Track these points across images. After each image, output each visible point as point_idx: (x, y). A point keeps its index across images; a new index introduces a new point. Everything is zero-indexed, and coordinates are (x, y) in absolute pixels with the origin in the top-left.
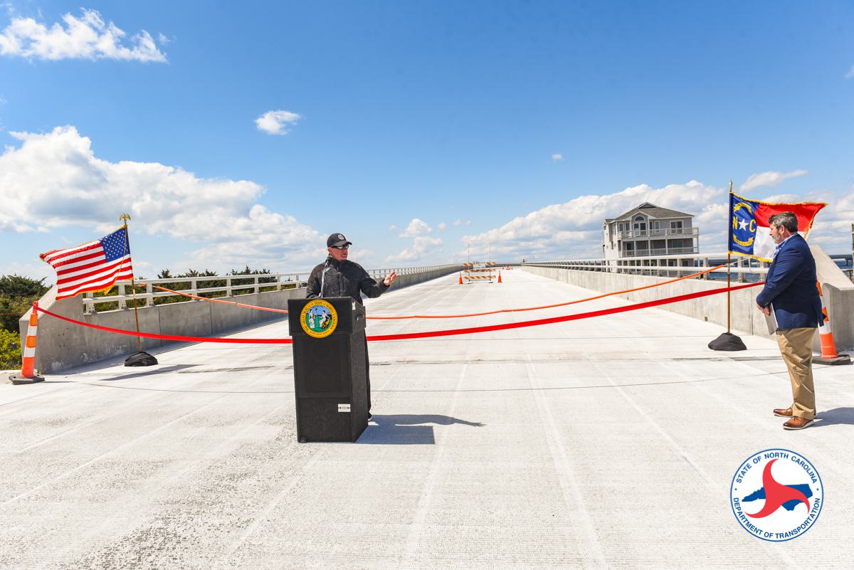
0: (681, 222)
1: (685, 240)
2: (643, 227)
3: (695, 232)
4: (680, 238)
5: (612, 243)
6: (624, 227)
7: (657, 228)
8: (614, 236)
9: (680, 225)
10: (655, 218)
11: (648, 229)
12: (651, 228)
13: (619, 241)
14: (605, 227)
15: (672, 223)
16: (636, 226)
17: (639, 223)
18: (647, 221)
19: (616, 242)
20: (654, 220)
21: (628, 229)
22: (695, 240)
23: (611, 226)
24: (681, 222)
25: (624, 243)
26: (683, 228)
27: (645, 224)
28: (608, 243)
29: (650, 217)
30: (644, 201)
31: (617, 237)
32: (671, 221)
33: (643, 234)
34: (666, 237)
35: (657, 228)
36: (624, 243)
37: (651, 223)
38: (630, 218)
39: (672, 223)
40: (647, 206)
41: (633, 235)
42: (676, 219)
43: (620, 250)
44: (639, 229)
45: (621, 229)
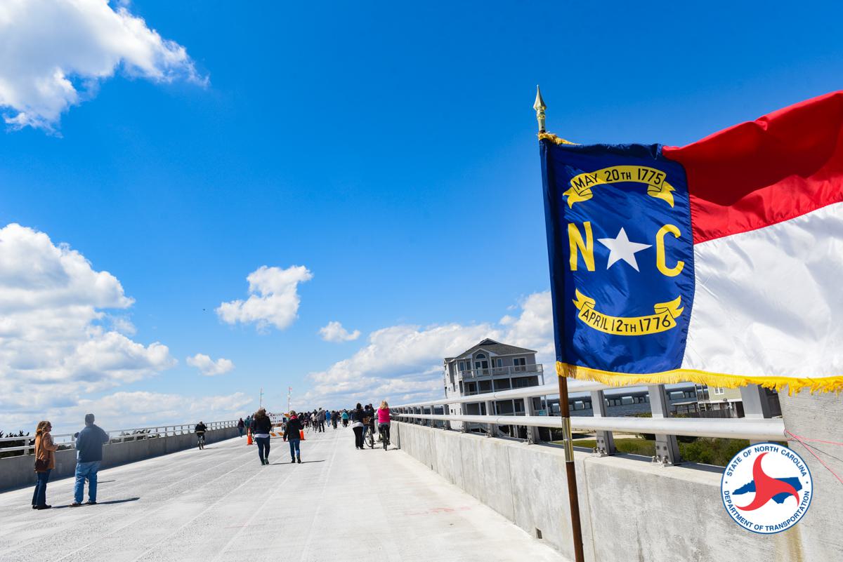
0: (524, 359)
1: (530, 378)
2: (485, 365)
3: (539, 368)
4: (524, 376)
5: (454, 384)
6: (465, 366)
7: (500, 365)
8: (455, 376)
9: (523, 361)
10: (497, 355)
11: (490, 368)
12: (493, 367)
13: (460, 382)
14: (445, 367)
15: (515, 360)
16: (478, 365)
17: (480, 360)
18: (488, 358)
19: (457, 383)
20: (496, 357)
21: (469, 368)
22: (540, 378)
23: (451, 365)
24: (524, 359)
25: (466, 383)
26: (526, 365)
27: (486, 362)
28: (450, 385)
29: (492, 354)
30: (483, 338)
31: (458, 377)
32: (513, 358)
33: (486, 373)
34: (510, 376)
35: (500, 365)
36: (466, 383)
37: (493, 361)
38: (470, 356)
39: (515, 360)
40: (488, 343)
41: (475, 375)
42: (518, 355)
43: (461, 391)
44: (480, 369)
45: (461, 368)
